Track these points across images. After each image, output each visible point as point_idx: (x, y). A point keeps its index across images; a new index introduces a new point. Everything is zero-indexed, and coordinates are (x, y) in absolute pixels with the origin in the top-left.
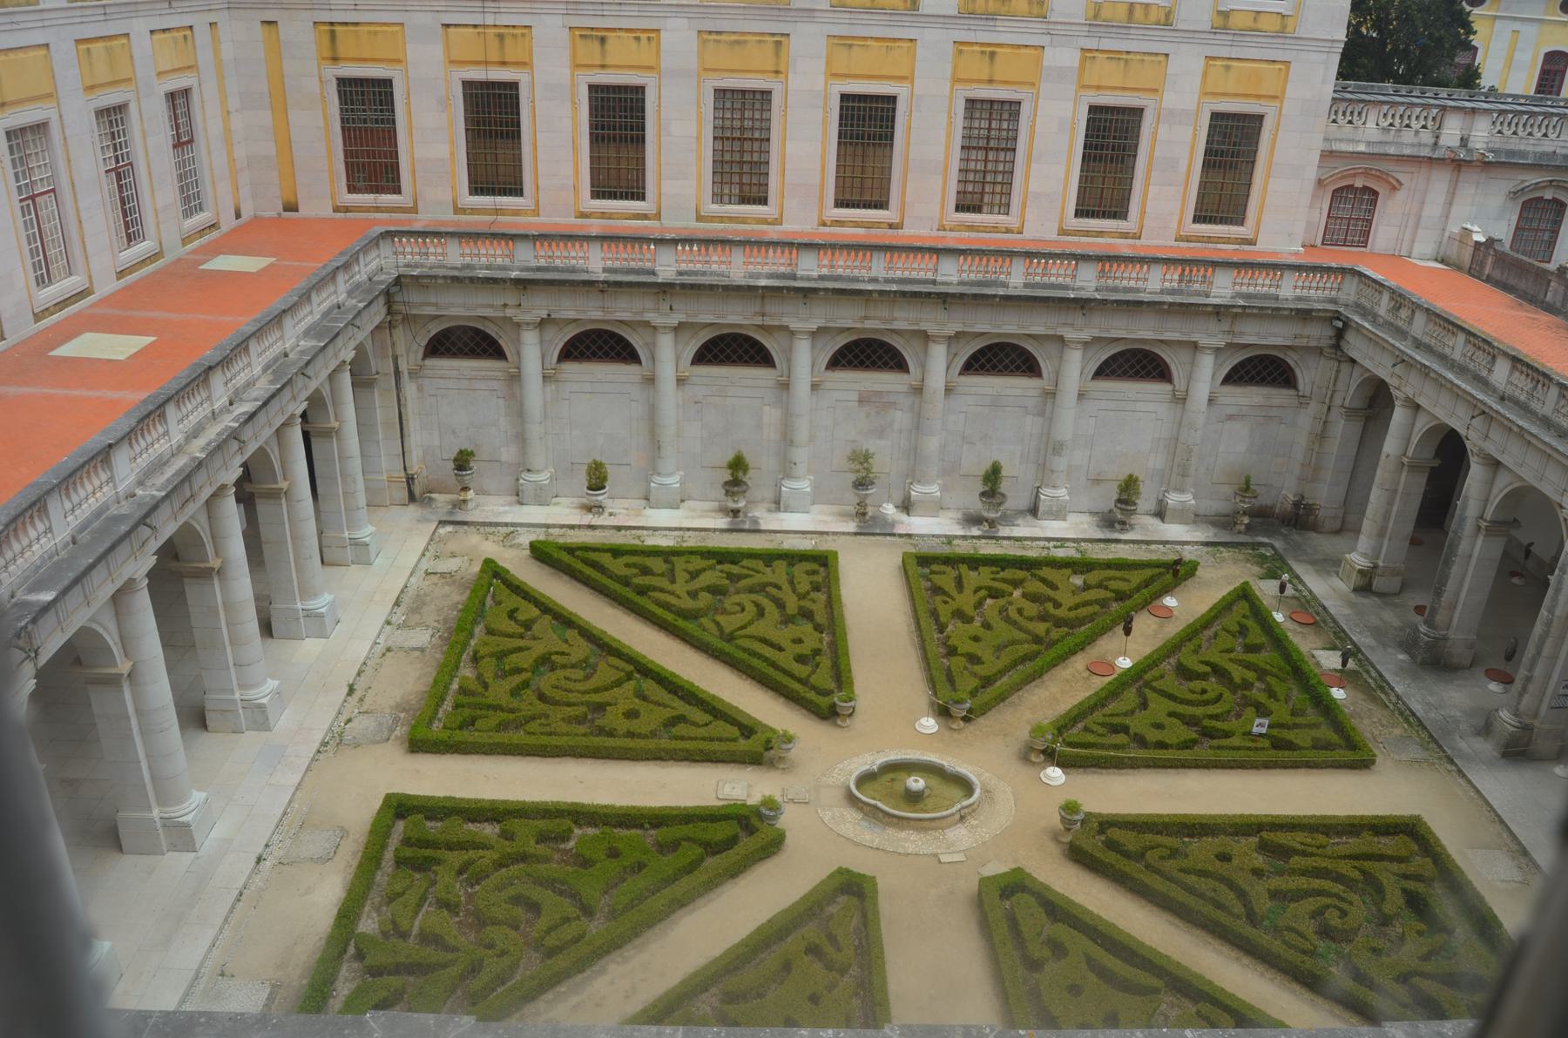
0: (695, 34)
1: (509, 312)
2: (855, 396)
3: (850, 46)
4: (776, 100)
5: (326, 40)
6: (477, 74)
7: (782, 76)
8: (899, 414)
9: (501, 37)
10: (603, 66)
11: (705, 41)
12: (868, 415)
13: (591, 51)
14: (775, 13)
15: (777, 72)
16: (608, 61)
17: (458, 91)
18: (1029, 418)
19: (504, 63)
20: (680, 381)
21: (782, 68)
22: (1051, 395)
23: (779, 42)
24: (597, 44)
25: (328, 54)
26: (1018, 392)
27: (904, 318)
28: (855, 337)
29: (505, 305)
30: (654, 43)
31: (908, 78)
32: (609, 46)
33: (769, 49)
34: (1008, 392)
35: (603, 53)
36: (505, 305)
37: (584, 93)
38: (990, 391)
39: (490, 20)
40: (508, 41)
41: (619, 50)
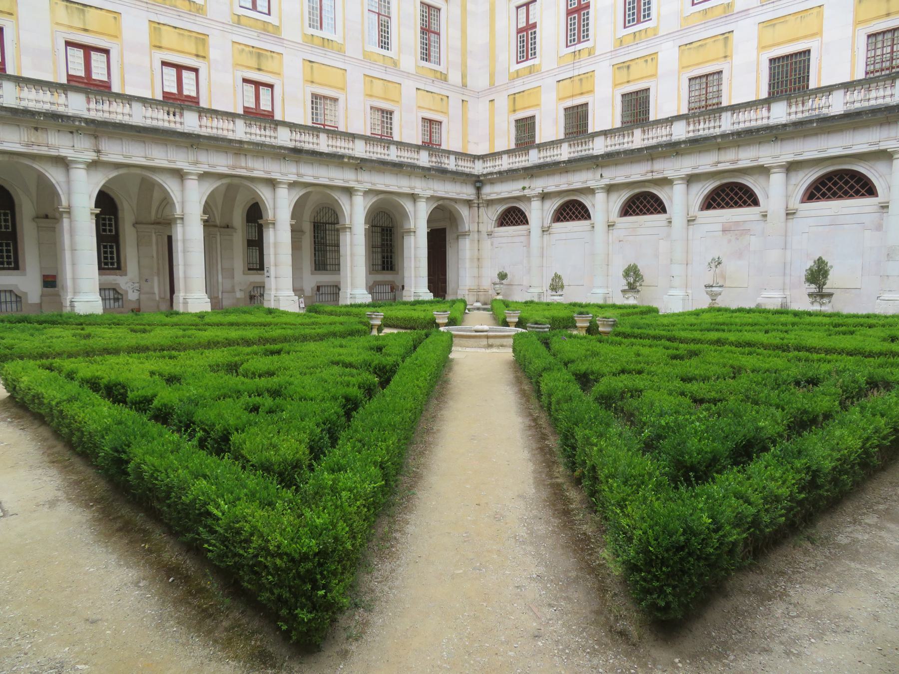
0: (677, 49)
1: (526, 192)
2: (719, 227)
3: (774, 25)
4: (725, 76)
5: (512, 103)
6: (569, 103)
7: (728, 59)
8: (753, 238)
9: (581, 80)
10: (628, 82)
11: (681, 53)
12: (729, 241)
13: (623, 75)
14: (724, 19)
15: (726, 57)
16: (631, 78)
17: (562, 113)
18: (867, 233)
19: (582, 94)
20: (611, 226)
21: (728, 54)
22: (885, 207)
23: (726, 36)
24: (625, 70)
25: (512, 109)
26: (855, 210)
27: (746, 157)
28: (717, 183)
29: (524, 188)
30: (654, 61)
31: (818, 33)
32: (632, 68)
33: (720, 44)
34: (845, 211)
35: (628, 74)
36: (524, 188)
37: (619, 99)
38: (828, 212)
39: (576, 73)
40: (584, 81)
41: (637, 70)
